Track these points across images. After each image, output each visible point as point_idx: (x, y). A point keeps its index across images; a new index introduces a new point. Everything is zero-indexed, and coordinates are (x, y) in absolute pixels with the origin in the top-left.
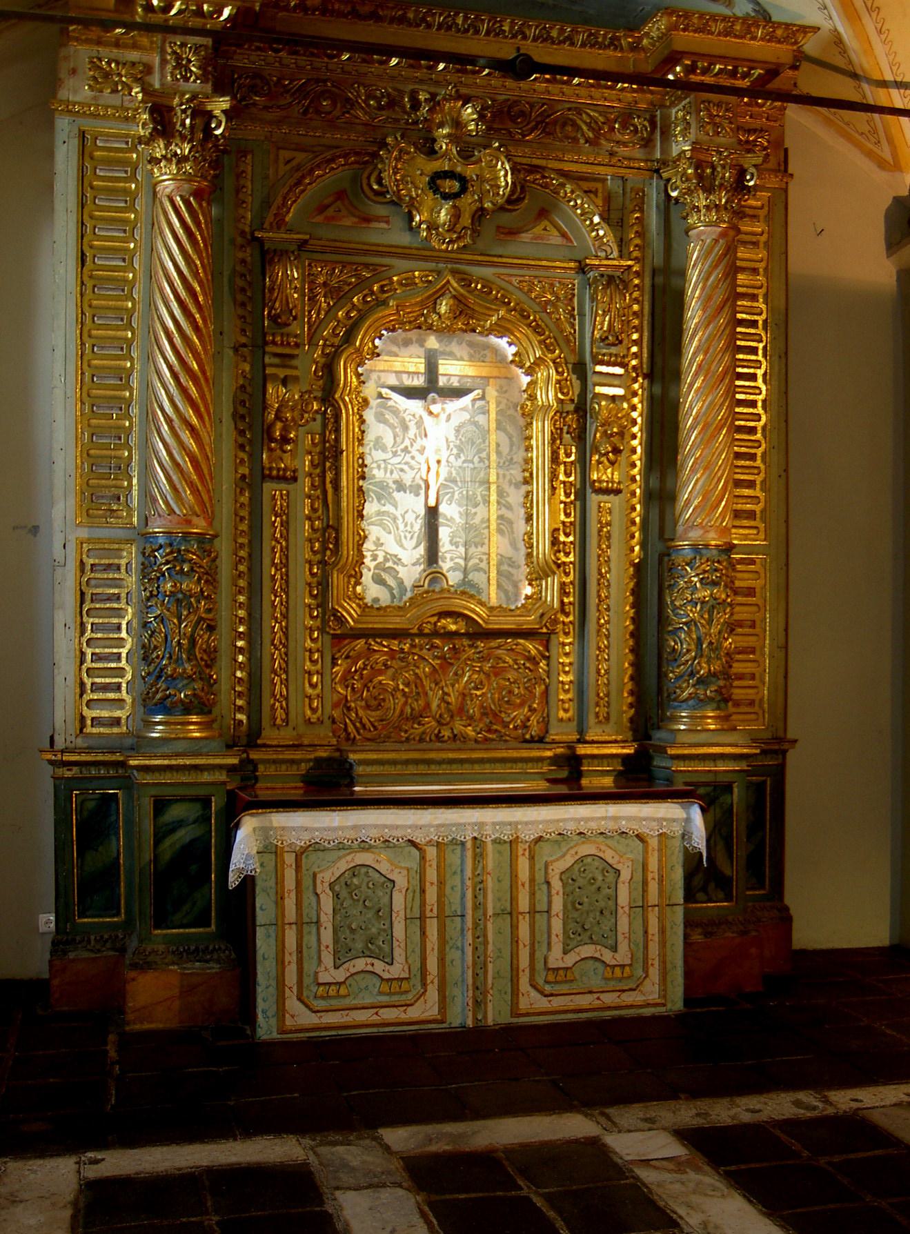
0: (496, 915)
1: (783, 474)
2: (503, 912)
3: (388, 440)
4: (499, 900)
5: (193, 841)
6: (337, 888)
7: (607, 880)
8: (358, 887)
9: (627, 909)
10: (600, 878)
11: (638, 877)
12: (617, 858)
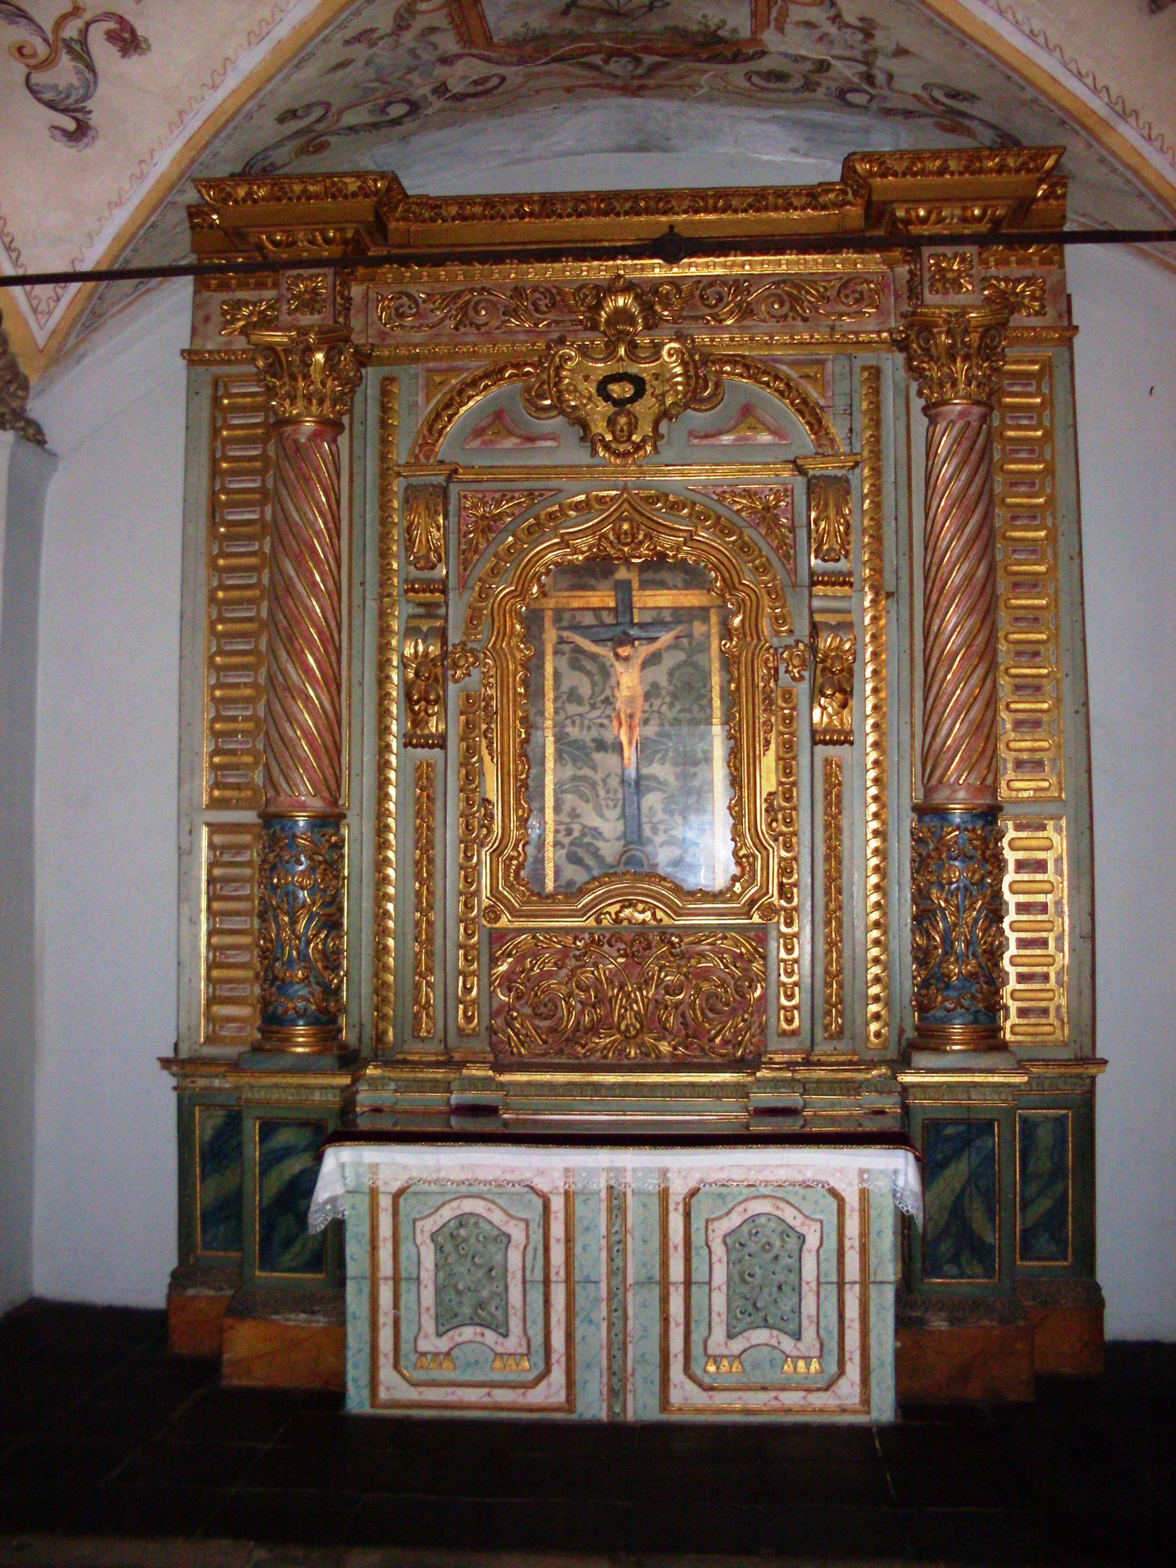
0: (640, 1284)
1: (1082, 710)
2: (650, 1280)
3: (585, 689)
4: (644, 1265)
5: (303, 1172)
6: (440, 1239)
7: (788, 1247)
8: (465, 1240)
9: (814, 1286)
10: (778, 1243)
11: (832, 1243)
12: (800, 1218)
